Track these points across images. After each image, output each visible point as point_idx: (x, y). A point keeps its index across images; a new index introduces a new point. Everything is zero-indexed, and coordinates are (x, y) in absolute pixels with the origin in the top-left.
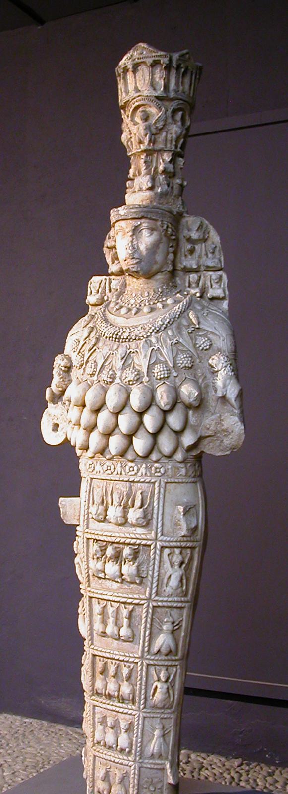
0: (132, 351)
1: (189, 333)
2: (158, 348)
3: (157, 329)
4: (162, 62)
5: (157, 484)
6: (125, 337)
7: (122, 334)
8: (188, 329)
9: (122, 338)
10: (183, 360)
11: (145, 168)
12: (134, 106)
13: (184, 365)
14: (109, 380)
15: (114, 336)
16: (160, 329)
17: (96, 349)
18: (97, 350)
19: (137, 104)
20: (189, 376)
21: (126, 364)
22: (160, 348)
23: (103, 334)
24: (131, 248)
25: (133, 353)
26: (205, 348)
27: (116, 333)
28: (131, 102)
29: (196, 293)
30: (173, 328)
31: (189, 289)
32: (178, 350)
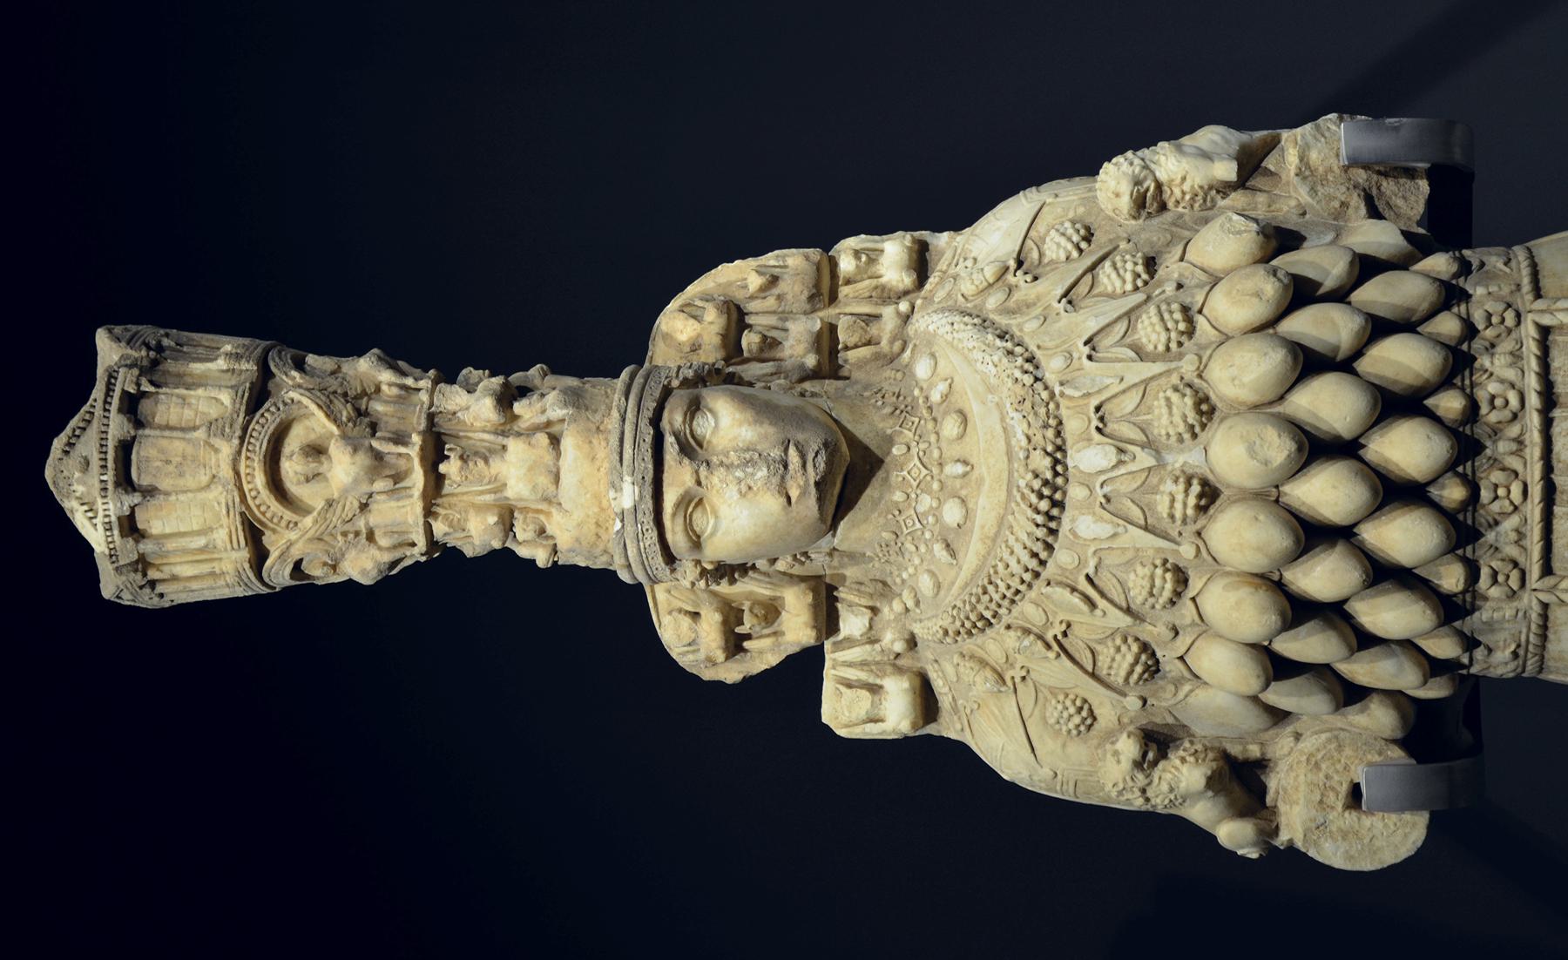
0: (1095, 423)
1: (1036, 279)
2: (1086, 344)
3: (1020, 360)
4: (132, 389)
5: (1546, 320)
6: (1048, 461)
7: (1037, 476)
8: (1022, 283)
9: (1049, 475)
11: (481, 463)
12: (266, 496)
14: (1196, 488)
15: (1044, 505)
17: (1088, 577)
18: (1091, 571)
19: (260, 480)
21: (1139, 437)
22: (1085, 338)
23: (1033, 564)
24: (750, 470)
25: (1102, 419)
26: (1082, 232)
27: (1034, 498)
28: (248, 507)
29: (898, 313)
31: (884, 343)
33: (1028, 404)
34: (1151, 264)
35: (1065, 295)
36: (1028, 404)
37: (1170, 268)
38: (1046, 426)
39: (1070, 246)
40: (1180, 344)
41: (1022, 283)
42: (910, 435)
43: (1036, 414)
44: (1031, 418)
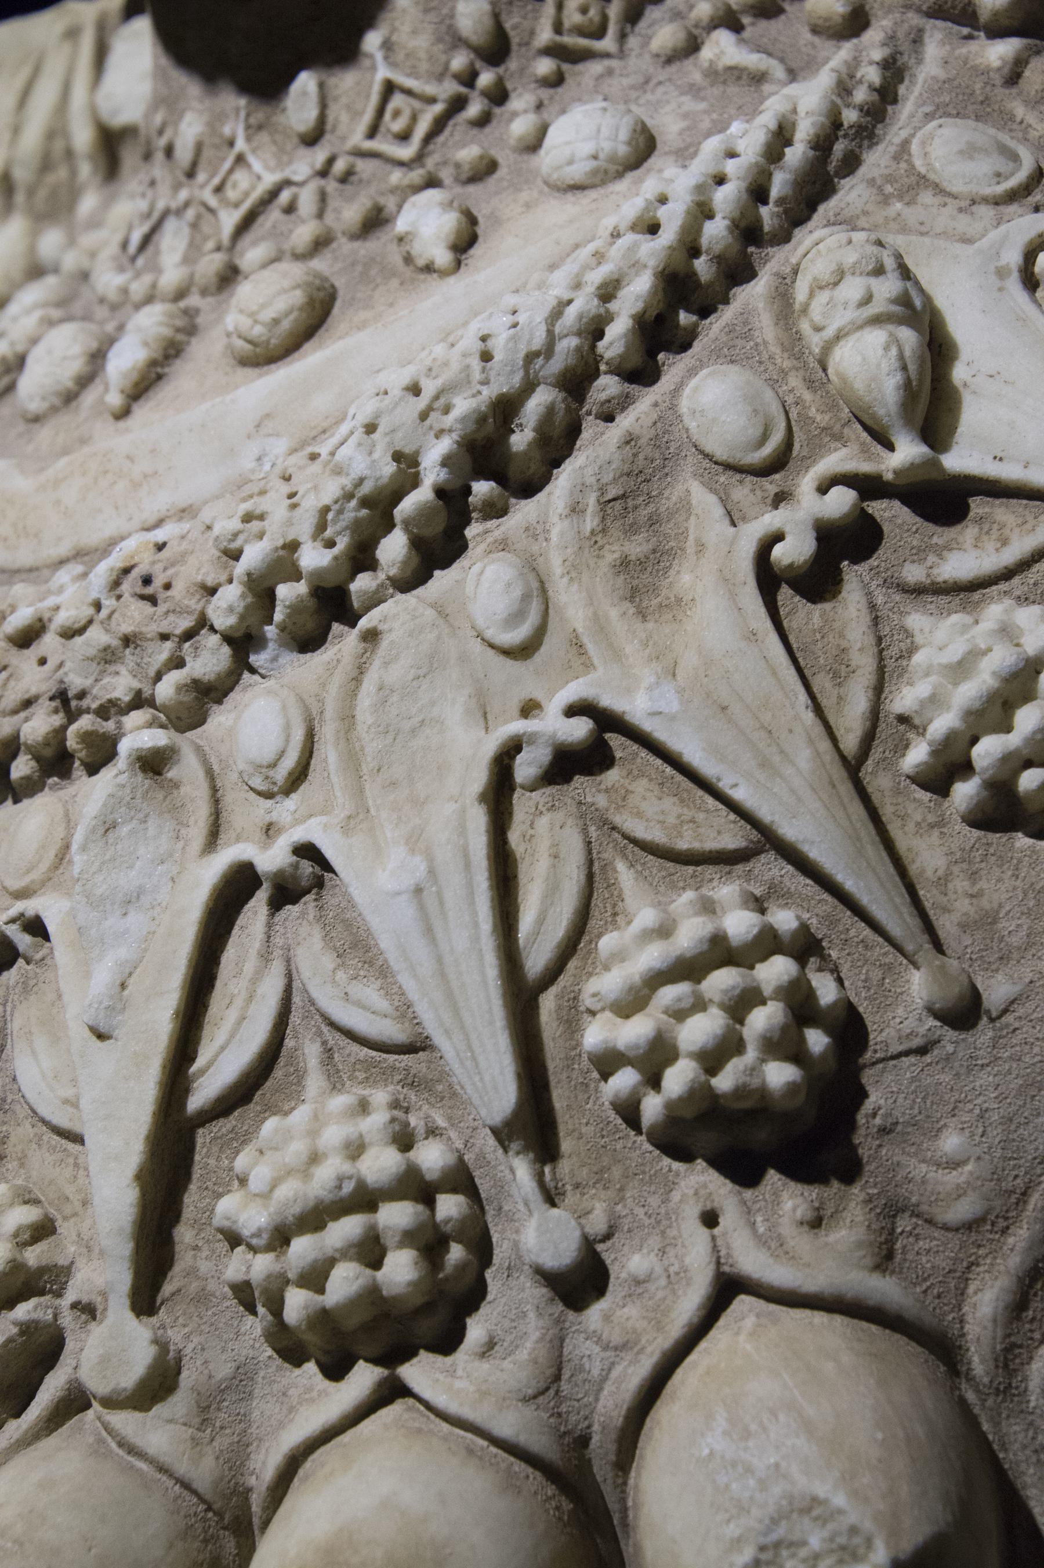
2: (307, 851)
8: (770, 520)
10: (655, 978)
13: (678, 1078)
16: (362, 558)
20: (773, 1244)
30: (535, 532)
32: (605, 844)
33: (133, 615)
34: (798, 1133)
35: (607, 722)
36: (133, 615)
37: (682, 1229)
38: (65, 701)
39: (943, 723)
40: (244, 1294)
41: (770, 520)
42: (357, 138)
43: (108, 657)
44: (97, 637)
